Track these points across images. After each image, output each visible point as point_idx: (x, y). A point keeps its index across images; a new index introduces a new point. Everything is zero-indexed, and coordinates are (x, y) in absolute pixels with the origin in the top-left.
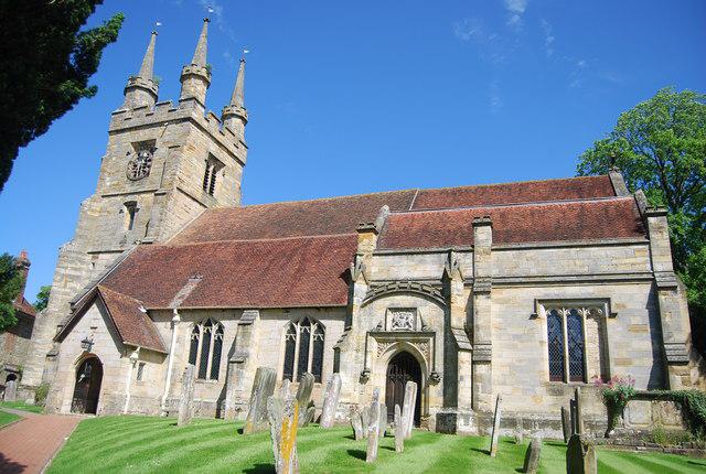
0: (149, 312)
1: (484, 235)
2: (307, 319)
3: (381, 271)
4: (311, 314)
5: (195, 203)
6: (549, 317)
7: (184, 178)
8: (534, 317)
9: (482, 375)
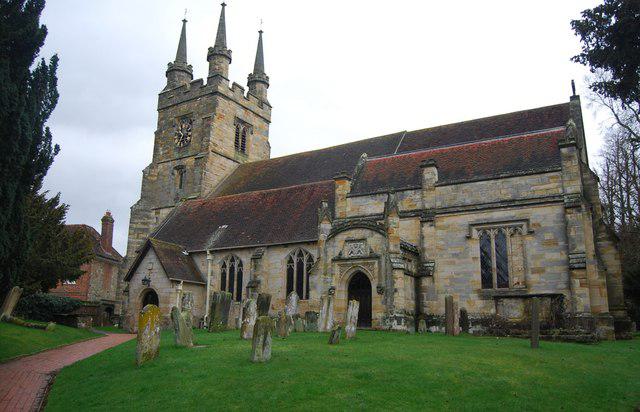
1: (431, 175)
4: (304, 247)
7: (217, 142)
8: (469, 238)
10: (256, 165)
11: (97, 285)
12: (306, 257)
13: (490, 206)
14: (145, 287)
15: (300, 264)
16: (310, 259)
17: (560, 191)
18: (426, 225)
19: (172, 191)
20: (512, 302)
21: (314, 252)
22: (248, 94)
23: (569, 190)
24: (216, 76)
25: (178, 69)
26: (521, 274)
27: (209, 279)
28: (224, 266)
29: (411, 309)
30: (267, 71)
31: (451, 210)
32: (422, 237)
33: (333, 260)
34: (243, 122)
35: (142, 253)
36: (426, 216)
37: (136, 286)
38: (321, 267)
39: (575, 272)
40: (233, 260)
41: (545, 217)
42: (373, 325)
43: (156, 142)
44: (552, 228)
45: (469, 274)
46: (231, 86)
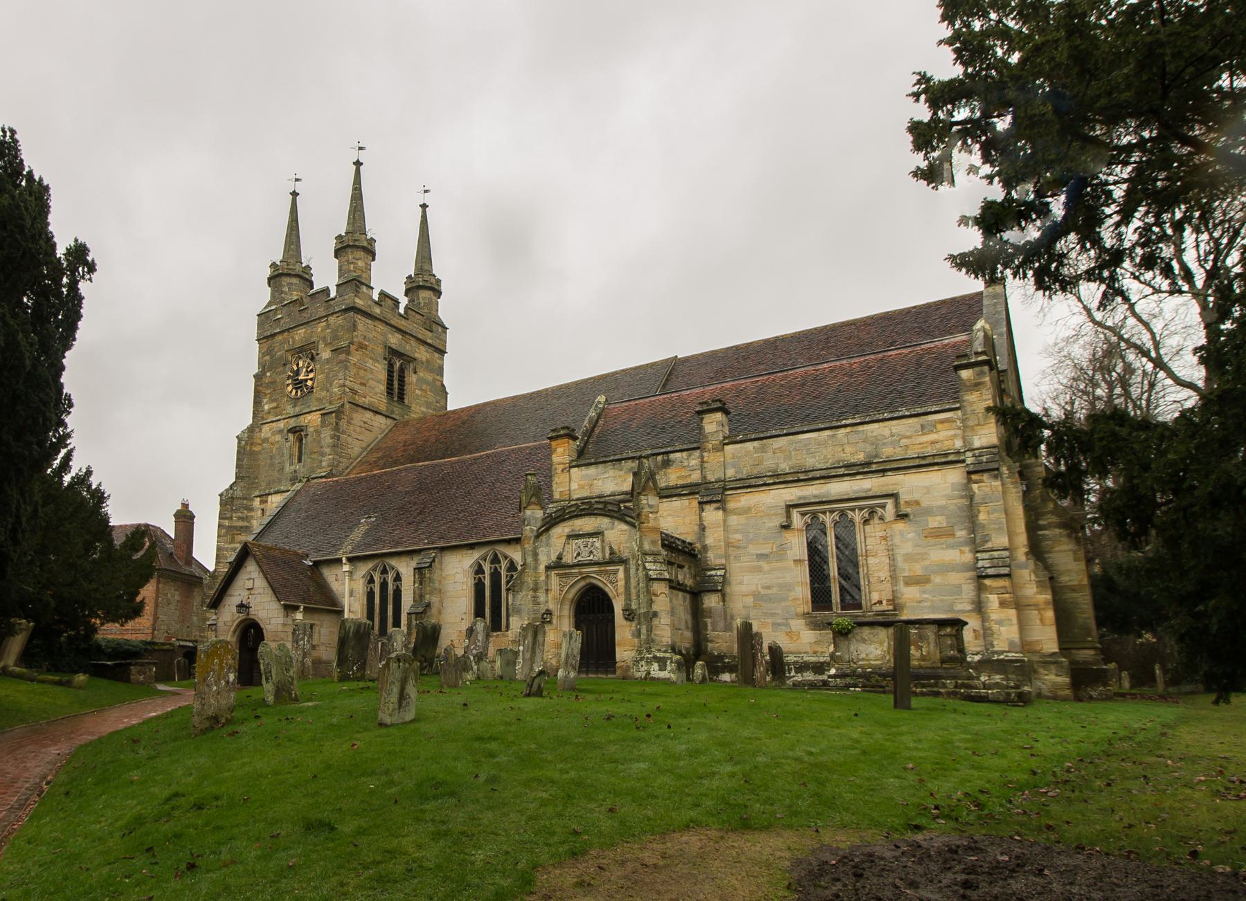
2: (496, 555)
4: (502, 549)
6: (808, 526)
8: (786, 527)
12: (504, 565)
13: (824, 473)
14: (242, 616)
15: (496, 576)
16: (512, 566)
18: (709, 509)
21: (516, 554)
24: (354, 282)
25: (288, 274)
26: (887, 587)
27: (346, 602)
31: (753, 482)
32: (703, 528)
33: (548, 568)
34: (400, 355)
35: (237, 567)
36: (711, 493)
37: (228, 616)
38: (529, 580)
39: (987, 582)
40: (384, 571)
44: (943, 507)
45: (789, 587)
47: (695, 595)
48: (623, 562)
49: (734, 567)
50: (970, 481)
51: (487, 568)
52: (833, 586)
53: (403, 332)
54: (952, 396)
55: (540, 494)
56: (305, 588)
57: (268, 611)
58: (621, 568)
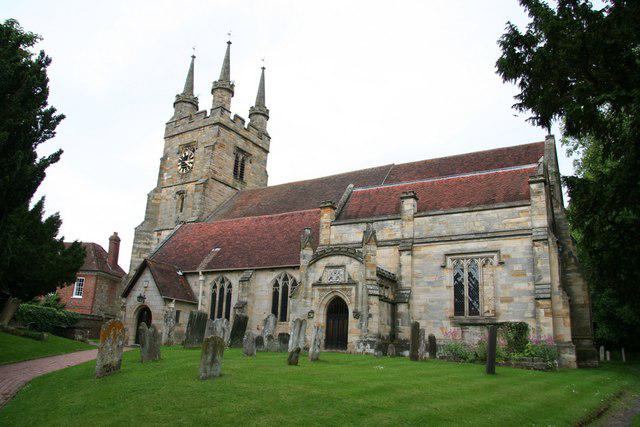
0: (184, 274)
1: (409, 205)
3: (336, 238)
5: (227, 188)
7: (216, 169)
8: (444, 267)
9: (401, 314)
10: (253, 192)
11: (75, 296)
12: (290, 281)
15: (285, 288)
16: (295, 283)
17: (529, 224)
18: (404, 254)
19: (174, 215)
20: (477, 330)
22: (250, 125)
23: (537, 224)
24: (221, 108)
25: (186, 100)
27: (200, 298)
28: (215, 287)
29: (386, 331)
30: (267, 104)
31: (428, 240)
33: (314, 285)
34: (242, 151)
35: (140, 272)
37: (132, 303)
38: (302, 291)
40: (223, 281)
41: (514, 249)
42: (349, 349)
43: (161, 168)
44: (522, 259)
45: (442, 302)
46: (232, 118)
47: (394, 304)
48: (355, 284)
49: (415, 289)
50: (534, 245)
51: (280, 283)
52: (466, 299)
53: (243, 137)
54: (516, 197)
55: (314, 240)
56: (175, 289)
57: (155, 301)
58: (354, 288)
